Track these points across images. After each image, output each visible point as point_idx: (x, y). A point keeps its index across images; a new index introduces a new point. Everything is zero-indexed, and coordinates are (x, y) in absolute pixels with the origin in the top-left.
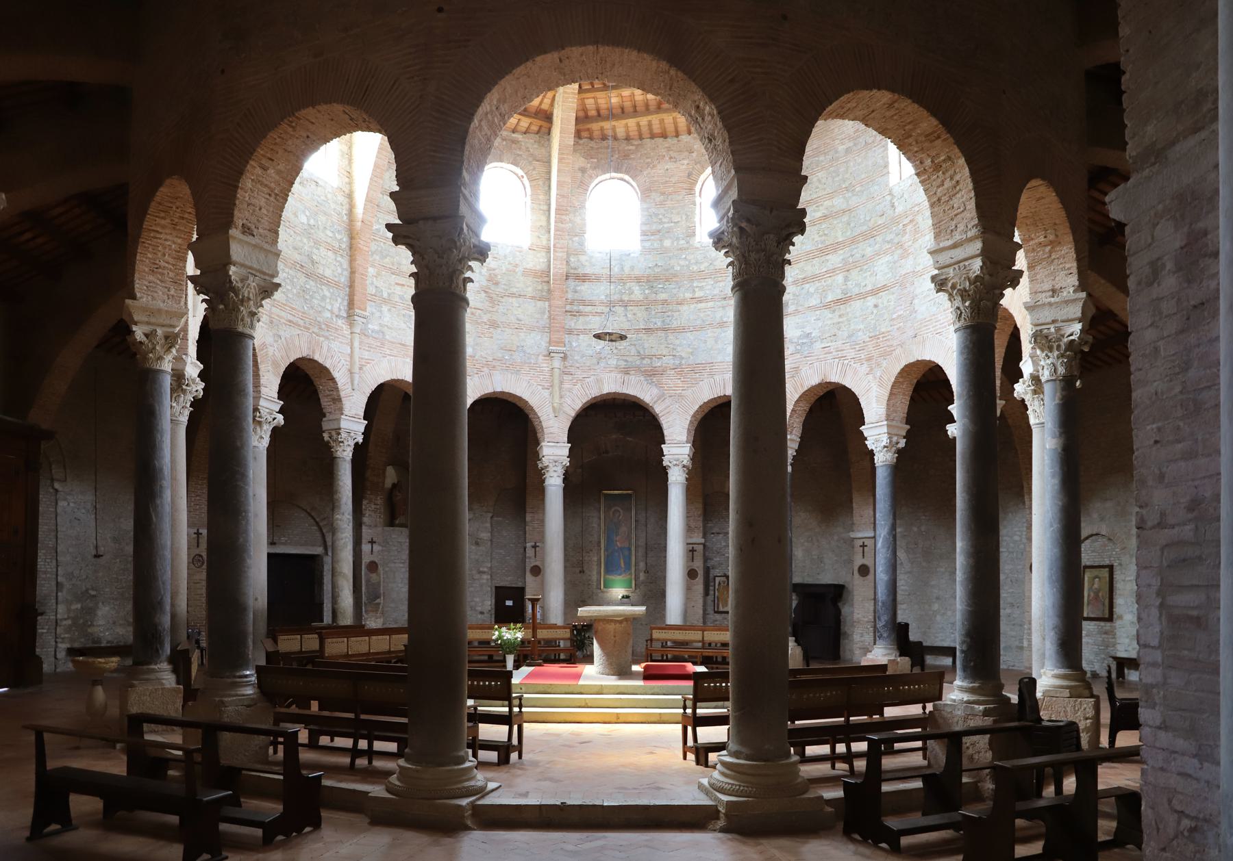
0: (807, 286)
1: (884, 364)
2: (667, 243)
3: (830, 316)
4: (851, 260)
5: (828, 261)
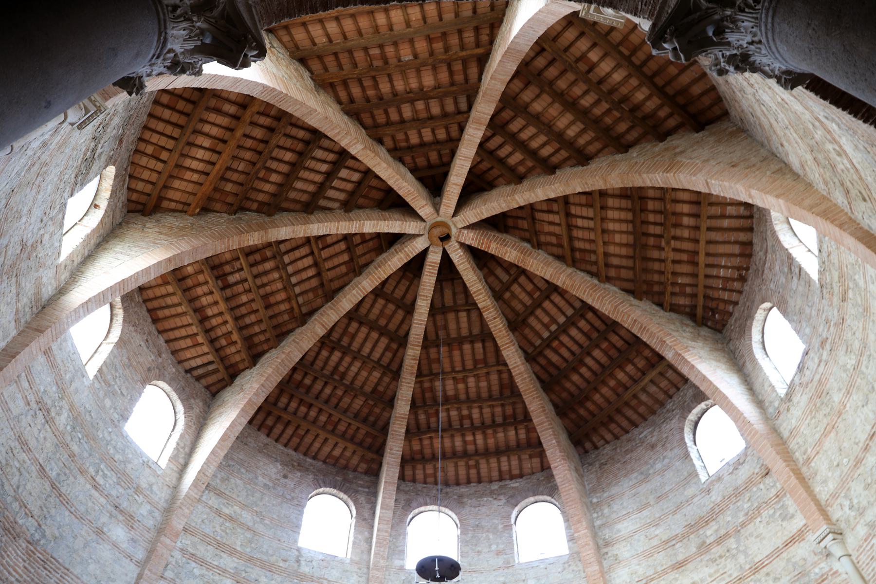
0: (193, 565)
2: (108, 403)
4: (244, 575)
5: (221, 557)
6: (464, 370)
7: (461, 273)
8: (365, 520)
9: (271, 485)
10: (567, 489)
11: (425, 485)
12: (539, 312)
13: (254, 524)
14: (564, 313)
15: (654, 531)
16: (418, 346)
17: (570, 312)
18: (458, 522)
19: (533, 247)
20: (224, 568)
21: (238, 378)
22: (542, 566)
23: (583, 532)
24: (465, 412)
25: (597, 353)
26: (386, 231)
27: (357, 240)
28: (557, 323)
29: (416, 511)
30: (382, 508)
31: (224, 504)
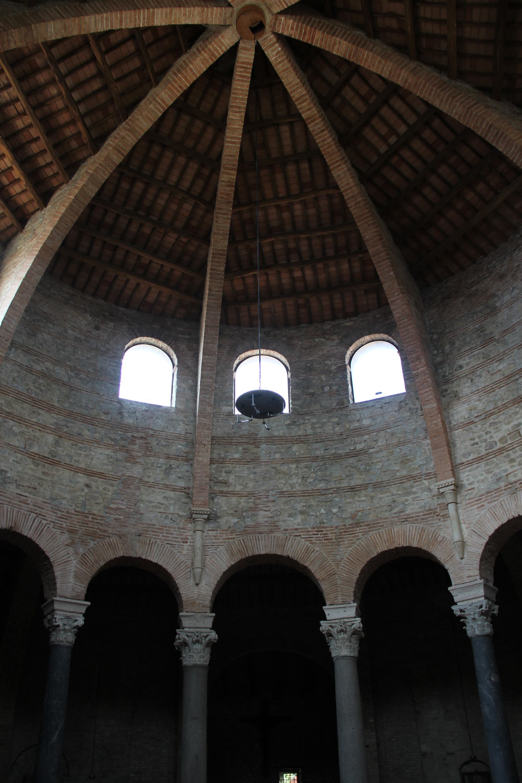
0: (11, 423)
1: (92, 544)
3: (32, 466)
5: (39, 414)
6: (289, 195)
7: (280, 75)
8: (188, 368)
9: (83, 338)
10: (406, 324)
11: (251, 329)
12: (375, 121)
13: (70, 379)
14: (405, 122)
15: (497, 366)
16: (232, 169)
17: (412, 119)
18: (288, 365)
19: (368, 35)
20: (43, 423)
21: (29, 223)
22: (377, 406)
23: (422, 368)
24: (292, 245)
25: (443, 170)
26: (183, 23)
27: (148, 37)
28: (398, 135)
29: (243, 356)
30: (204, 354)
31: (34, 361)
